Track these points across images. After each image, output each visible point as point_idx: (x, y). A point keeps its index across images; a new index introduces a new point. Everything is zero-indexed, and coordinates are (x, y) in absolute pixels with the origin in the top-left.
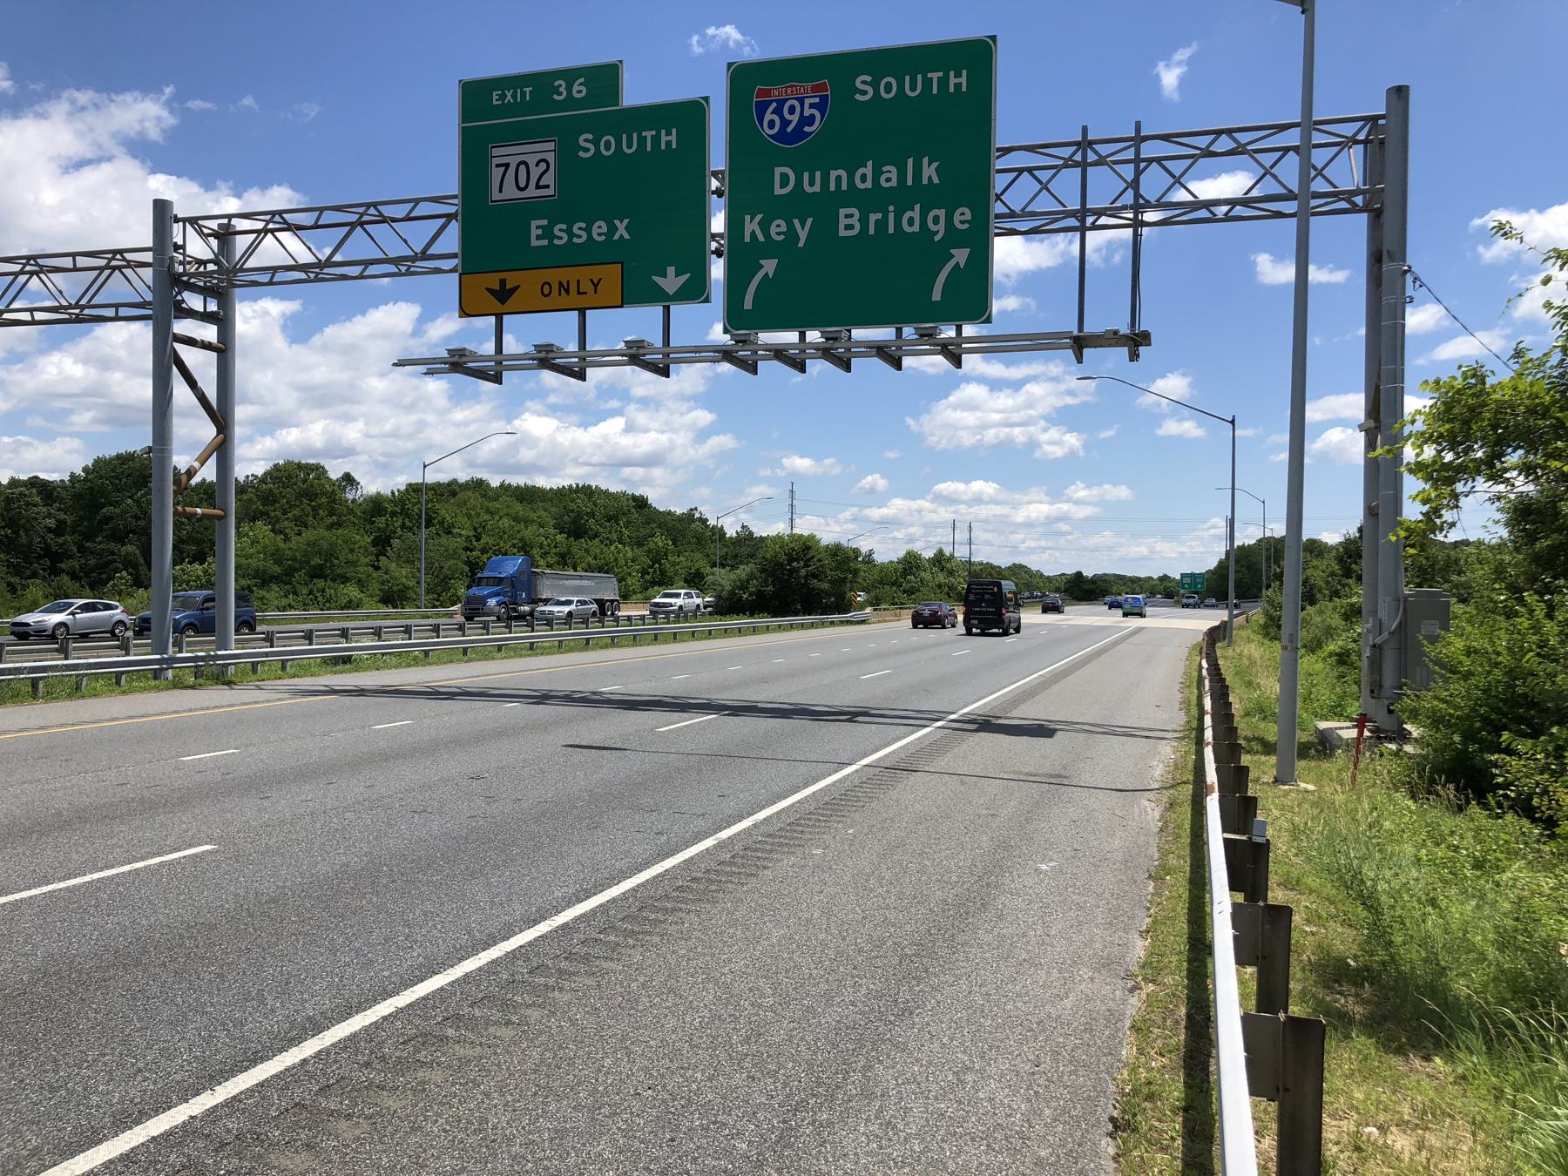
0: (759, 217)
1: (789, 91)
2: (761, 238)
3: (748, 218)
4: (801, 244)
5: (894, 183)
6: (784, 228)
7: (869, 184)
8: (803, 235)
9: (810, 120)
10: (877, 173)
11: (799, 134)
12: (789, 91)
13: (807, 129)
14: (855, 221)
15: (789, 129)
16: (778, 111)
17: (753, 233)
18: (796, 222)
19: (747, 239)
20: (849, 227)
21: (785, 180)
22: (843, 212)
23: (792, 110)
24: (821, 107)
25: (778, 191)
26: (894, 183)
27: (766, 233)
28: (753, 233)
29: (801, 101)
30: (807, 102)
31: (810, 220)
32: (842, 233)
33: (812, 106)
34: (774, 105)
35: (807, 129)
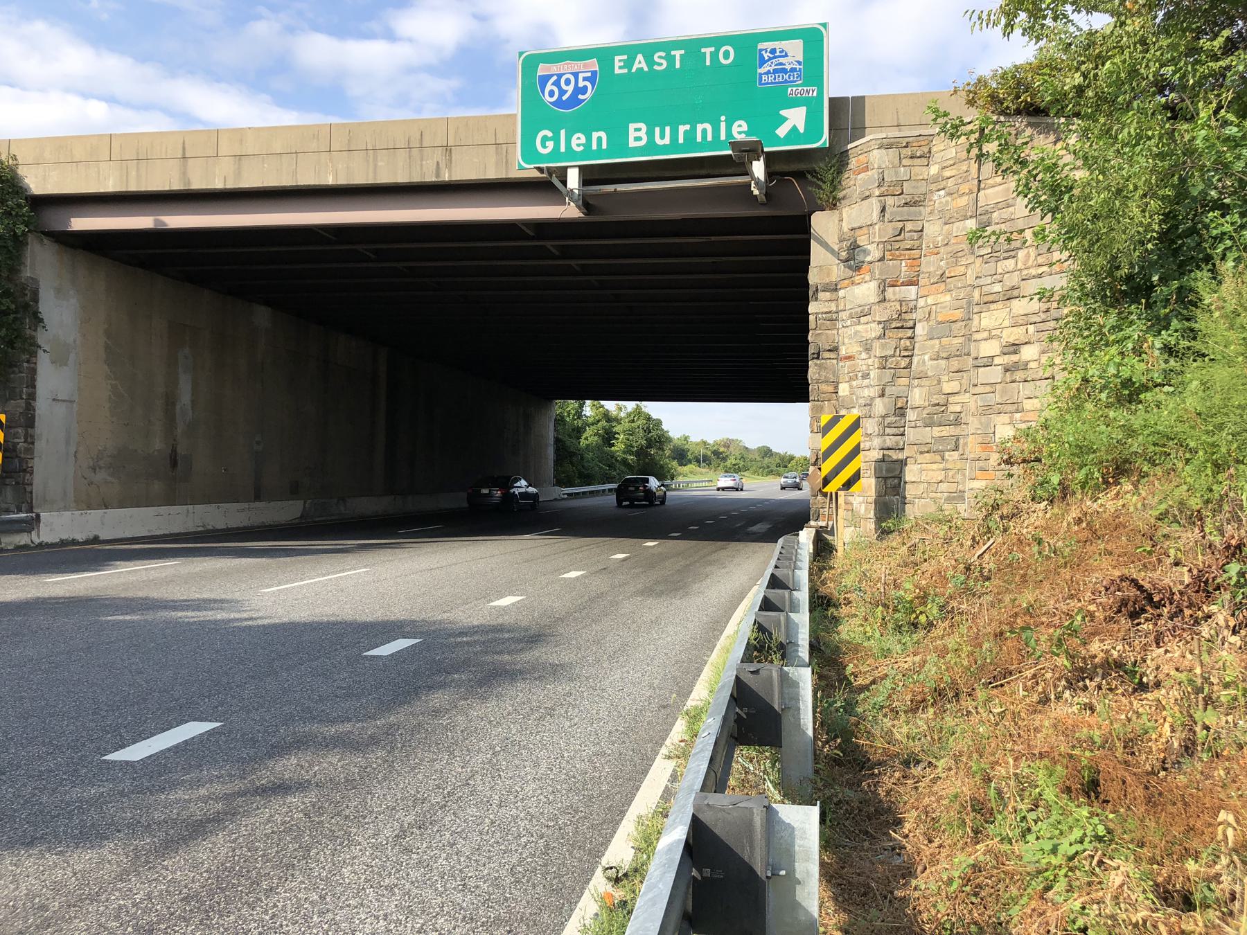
6: (583, 140)
11: (574, 101)
14: (643, 134)
15: (564, 98)
20: (638, 139)
22: (632, 126)
23: (568, 82)
29: (576, 75)
30: (581, 76)
32: (632, 144)
34: (555, 78)
35: (581, 97)
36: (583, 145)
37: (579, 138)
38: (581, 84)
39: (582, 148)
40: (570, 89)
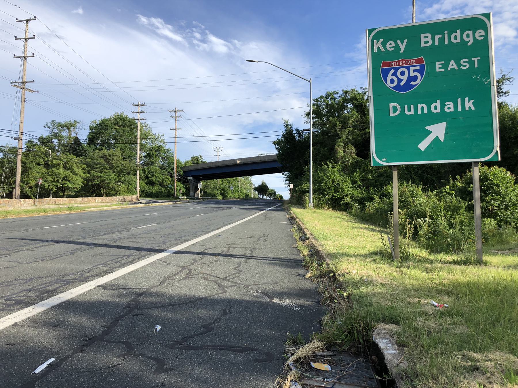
5: (452, 110)
7: (438, 111)
9: (415, 78)
10: (443, 106)
11: (408, 86)
12: (401, 63)
13: (413, 83)
16: (395, 74)
21: (395, 109)
23: (403, 73)
24: (421, 71)
25: (391, 114)
26: (452, 110)
29: (408, 68)
30: (412, 69)
33: (415, 71)
34: (393, 71)
38: (412, 74)
40: (405, 78)
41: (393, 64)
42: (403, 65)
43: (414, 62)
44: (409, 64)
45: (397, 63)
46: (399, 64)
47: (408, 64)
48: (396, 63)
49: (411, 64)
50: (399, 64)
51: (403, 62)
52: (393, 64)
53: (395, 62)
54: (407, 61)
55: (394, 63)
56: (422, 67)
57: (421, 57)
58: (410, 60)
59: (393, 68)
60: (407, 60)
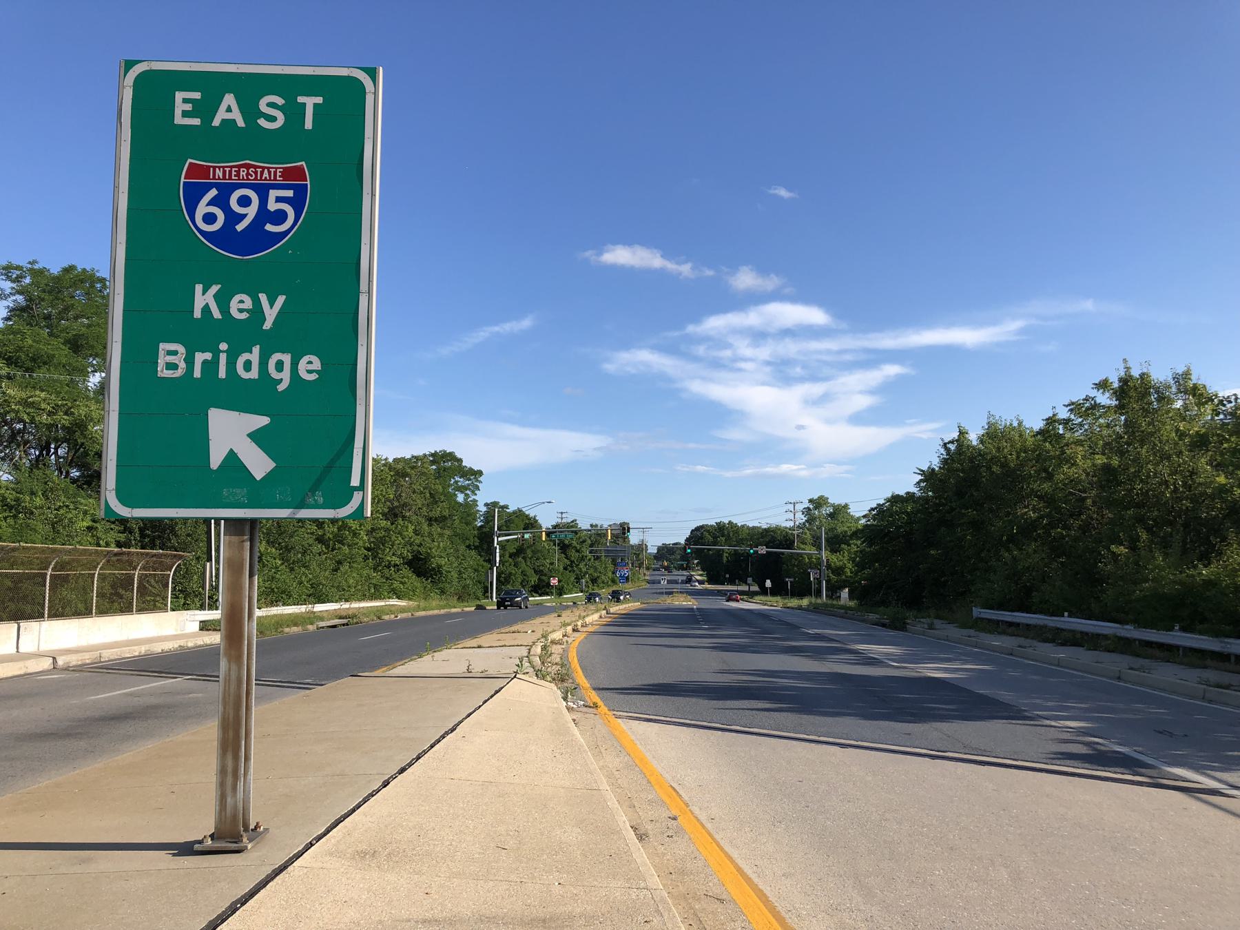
0: (215, 289)
1: (243, 173)
2: (217, 314)
3: (199, 288)
4: (268, 325)
6: (248, 304)
8: (271, 314)
11: (257, 238)
12: (243, 173)
16: (221, 201)
17: (206, 310)
18: (263, 298)
19: (197, 314)
27: (225, 310)
28: (206, 310)
29: (262, 191)
30: (273, 194)
31: (281, 300)
36: (247, 311)
37: (242, 302)
38: (272, 206)
39: (244, 316)
40: (252, 211)
41: (219, 173)
42: (248, 179)
43: (278, 174)
44: (266, 179)
45: (234, 173)
46: (238, 175)
47: (261, 180)
48: (230, 172)
49: (270, 180)
50: (238, 175)
51: (248, 171)
52: (219, 173)
53: (227, 169)
54: (259, 170)
55: (224, 172)
56: (300, 191)
57: (300, 163)
58: (268, 168)
59: (217, 186)
60: (259, 167)
